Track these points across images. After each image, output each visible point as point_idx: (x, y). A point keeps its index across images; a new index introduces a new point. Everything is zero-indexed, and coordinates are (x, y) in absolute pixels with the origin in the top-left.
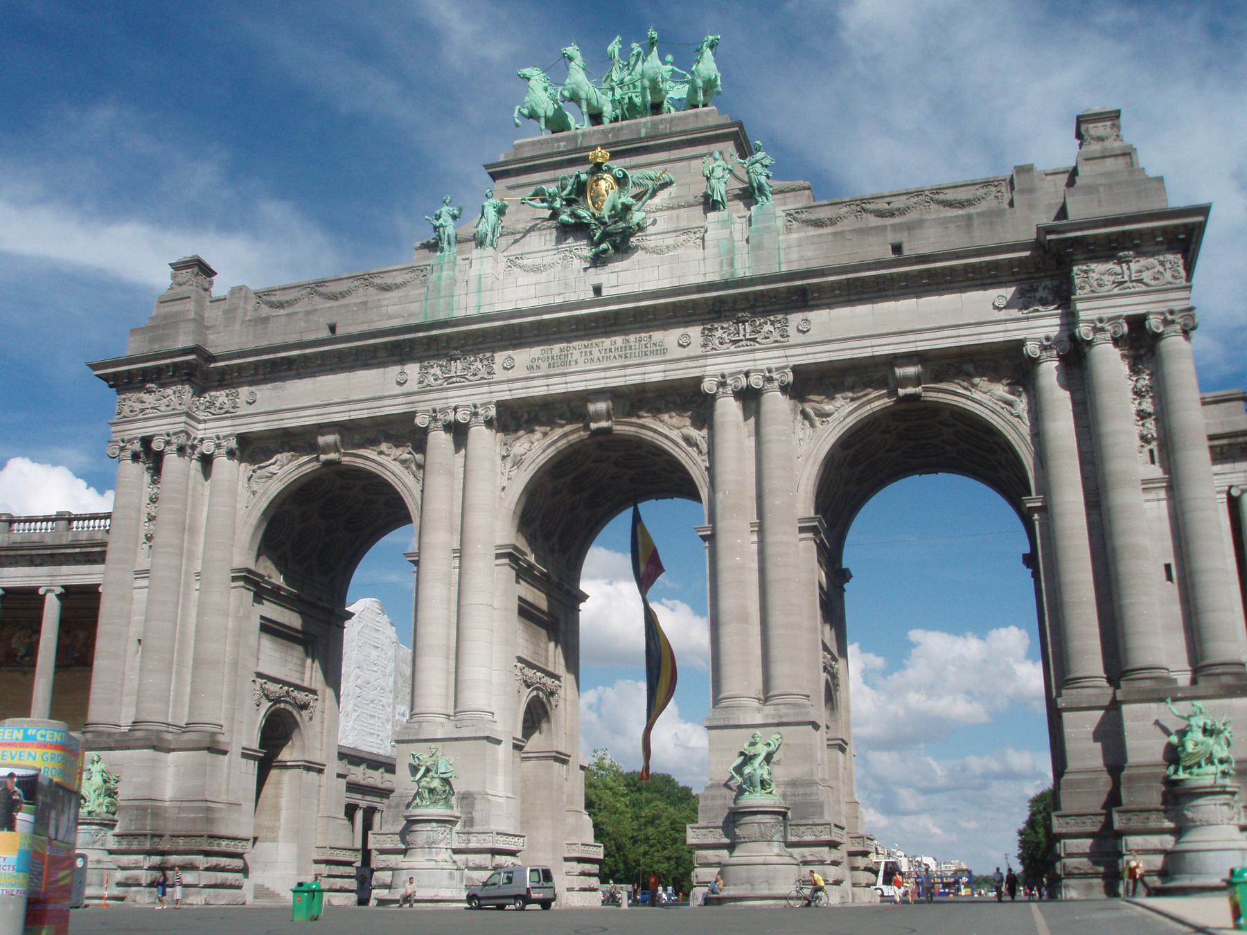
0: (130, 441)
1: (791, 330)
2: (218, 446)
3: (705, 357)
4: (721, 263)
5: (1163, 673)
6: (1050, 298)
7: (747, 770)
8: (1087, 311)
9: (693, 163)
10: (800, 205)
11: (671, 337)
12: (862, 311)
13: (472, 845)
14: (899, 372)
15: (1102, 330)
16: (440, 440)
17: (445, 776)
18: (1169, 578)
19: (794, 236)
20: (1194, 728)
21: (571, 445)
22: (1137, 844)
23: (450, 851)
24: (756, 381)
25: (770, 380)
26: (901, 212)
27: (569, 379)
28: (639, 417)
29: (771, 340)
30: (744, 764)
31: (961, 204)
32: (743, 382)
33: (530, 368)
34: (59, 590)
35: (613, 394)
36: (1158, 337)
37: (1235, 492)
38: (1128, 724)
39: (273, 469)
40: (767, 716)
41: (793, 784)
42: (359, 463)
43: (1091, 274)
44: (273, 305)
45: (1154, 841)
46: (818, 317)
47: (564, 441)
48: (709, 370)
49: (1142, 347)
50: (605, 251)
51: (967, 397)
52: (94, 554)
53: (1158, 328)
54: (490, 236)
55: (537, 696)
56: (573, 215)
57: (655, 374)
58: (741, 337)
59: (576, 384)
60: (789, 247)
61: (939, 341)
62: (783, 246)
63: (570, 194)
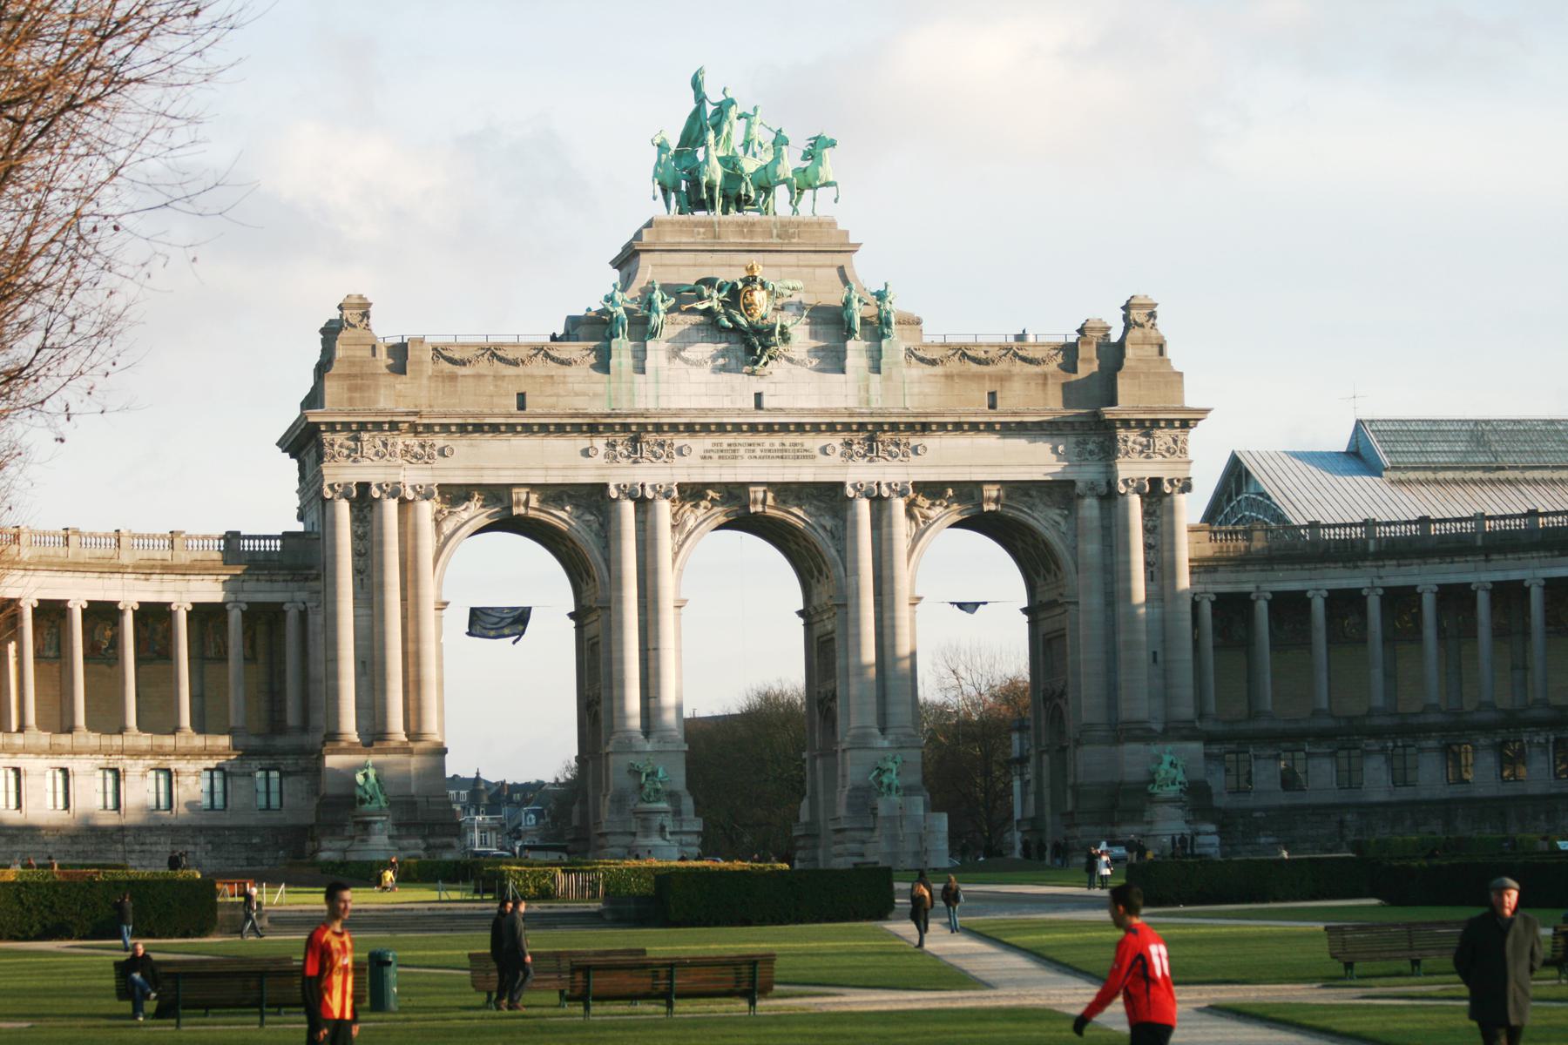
0: (347, 485)
5: (1148, 725)
6: (1097, 451)
9: (818, 271)
13: (685, 829)
18: (1155, 660)
27: (738, 471)
30: (879, 775)
34: (244, 607)
35: (769, 485)
37: (1197, 598)
39: (465, 516)
45: (1137, 829)
50: (766, 364)
51: (1029, 515)
56: (730, 319)
60: (912, 382)
62: (907, 381)
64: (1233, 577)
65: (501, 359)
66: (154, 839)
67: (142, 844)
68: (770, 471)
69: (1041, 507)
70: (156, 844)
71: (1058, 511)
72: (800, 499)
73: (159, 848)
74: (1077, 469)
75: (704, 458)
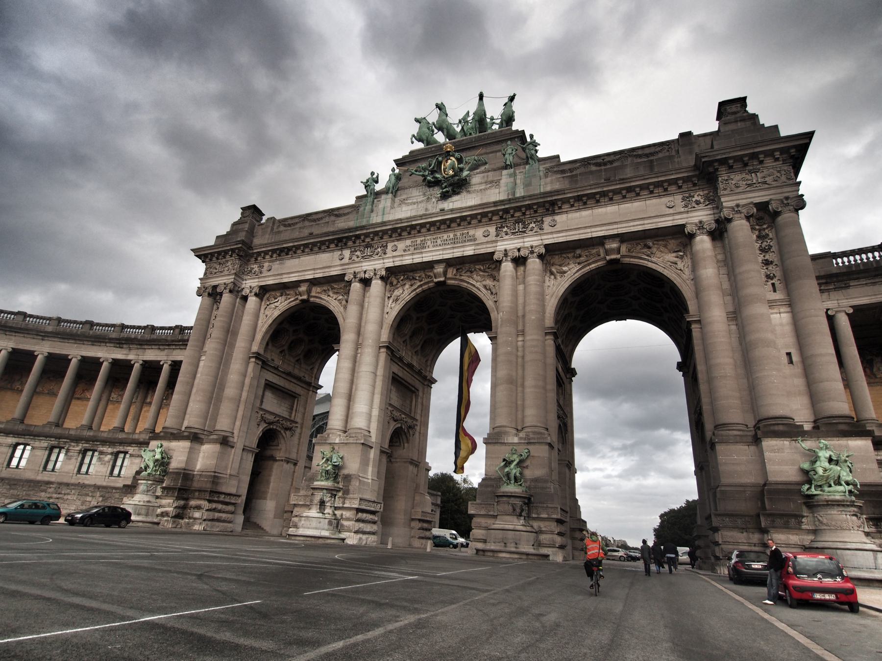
1: (546, 226)
2: (251, 292)
3: (496, 241)
4: (508, 194)
6: (702, 201)
7: (507, 470)
8: (728, 202)
10: (553, 164)
11: (479, 233)
12: (585, 213)
13: (345, 506)
14: (607, 246)
15: (739, 212)
16: (356, 286)
17: (335, 464)
18: (791, 362)
19: (549, 179)
20: (822, 459)
21: (423, 291)
22: (780, 540)
23: (333, 508)
24: (523, 253)
25: (532, 252)
26: (611, 162)
27: (424, 255)
28: (461, 276)
29: (534, 231)
30: (506, 466)
31: (647, 155)
32: (517, 254)
33: (405, 251)
35: (449, 263)
36: (777, 214)
37: (829, 312)
38: (767, 454)
39: (276, 304)
40: (521, 438)
41: (536, 480)
42: (318, 301)
43: (730, 181)
44: (285, 226)
46: (561, 219)
47: (421, 289)
48: (498, 248)
49: (765, 224)
50: (447, 192)
52: (182, 343)
53: (778, 208)
54: (391, 188)
55: (401, 427)
57: (469, 251)
58: (517, 230)
59: (427, 257)
61: (632, 228)
63: (433, 168)
64: (869, 289)
65: (308, 220)
66: (69, 491)
67: (59, 494)
68: (444, 252)
69: (658, 254)
70: (68, 494)
71: (674, 255)
72: (471, 272)
73: (69, 497)
74: (685, 215)
75: (405, 251)
